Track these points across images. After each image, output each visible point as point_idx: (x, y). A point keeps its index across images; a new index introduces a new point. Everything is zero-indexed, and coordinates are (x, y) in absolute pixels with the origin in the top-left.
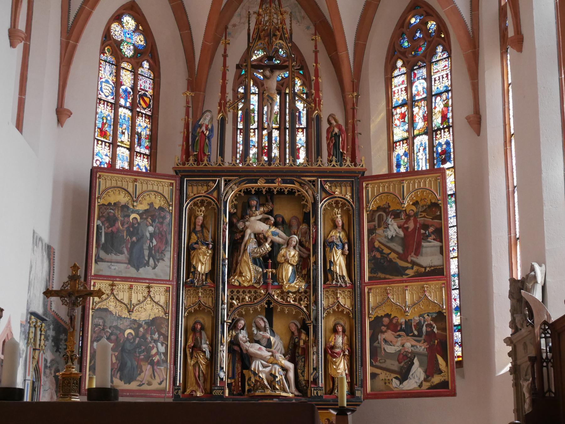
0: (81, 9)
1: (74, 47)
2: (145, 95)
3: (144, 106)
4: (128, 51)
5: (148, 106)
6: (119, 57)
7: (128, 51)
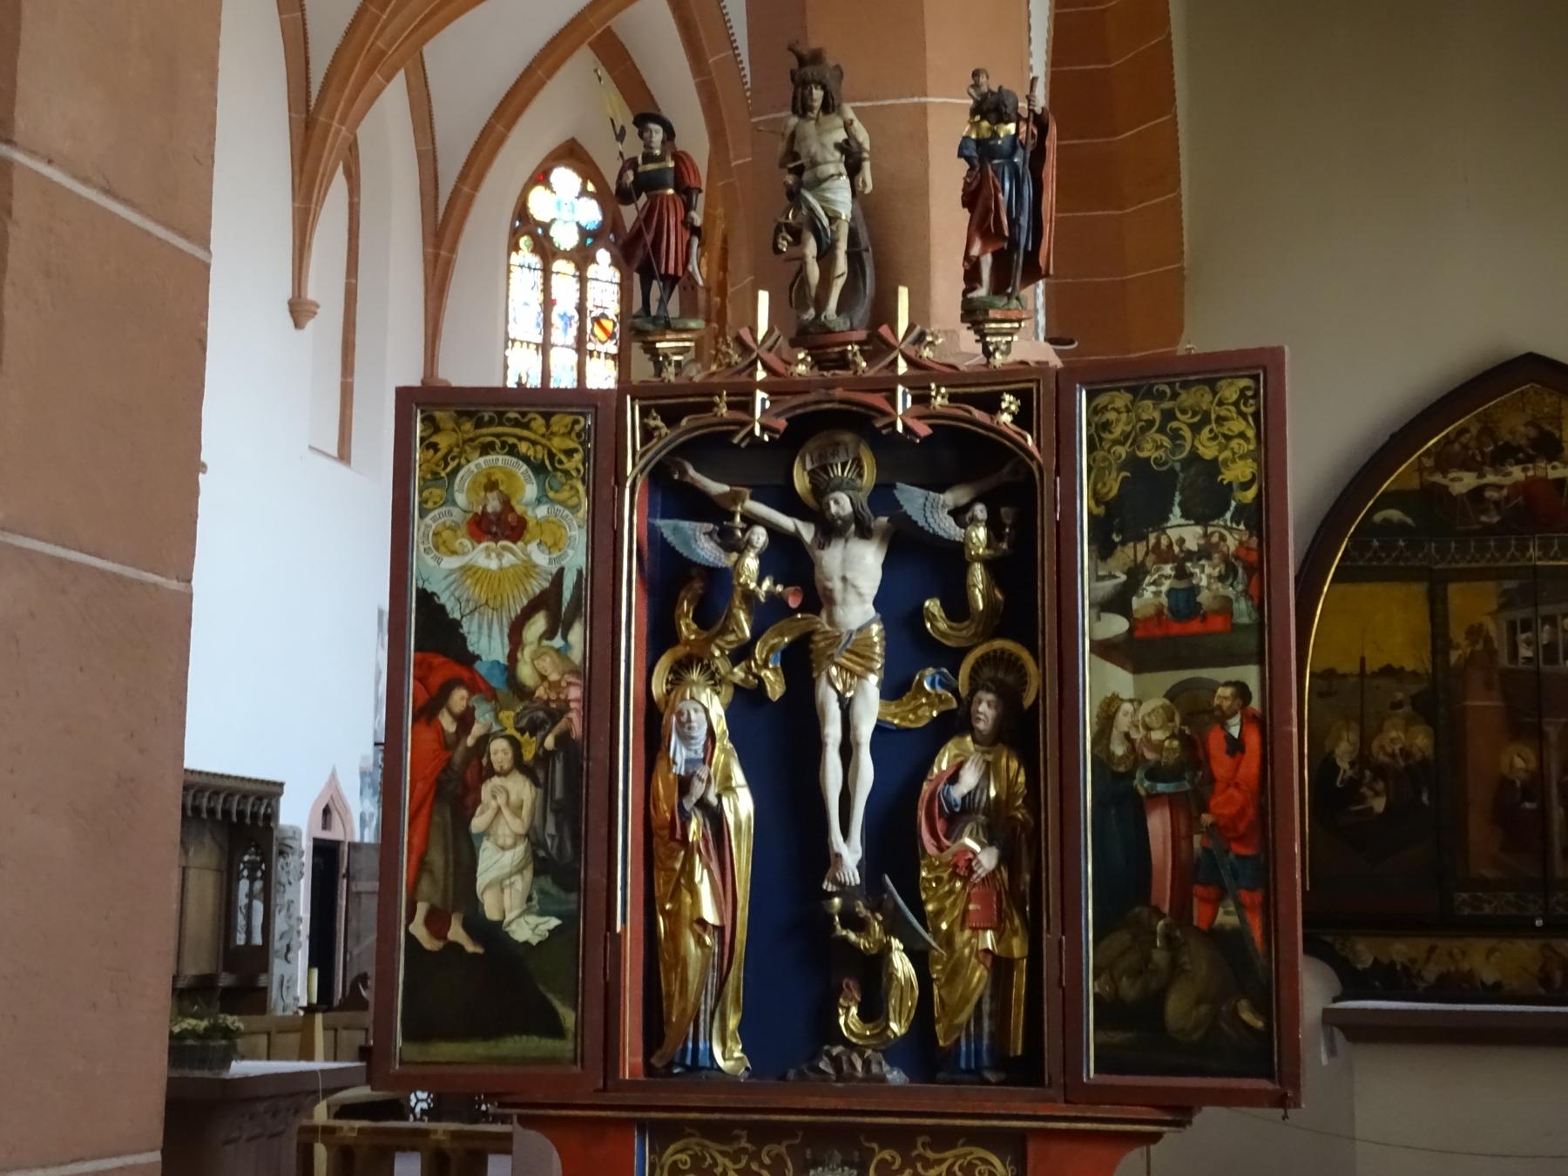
0: (456, 191)
1: (449, 264)
2: (604, 316)
3: (602, 336)
4: (566, 238)
5: (611, 336)
6: (546, 251)
7: (566, 238)
